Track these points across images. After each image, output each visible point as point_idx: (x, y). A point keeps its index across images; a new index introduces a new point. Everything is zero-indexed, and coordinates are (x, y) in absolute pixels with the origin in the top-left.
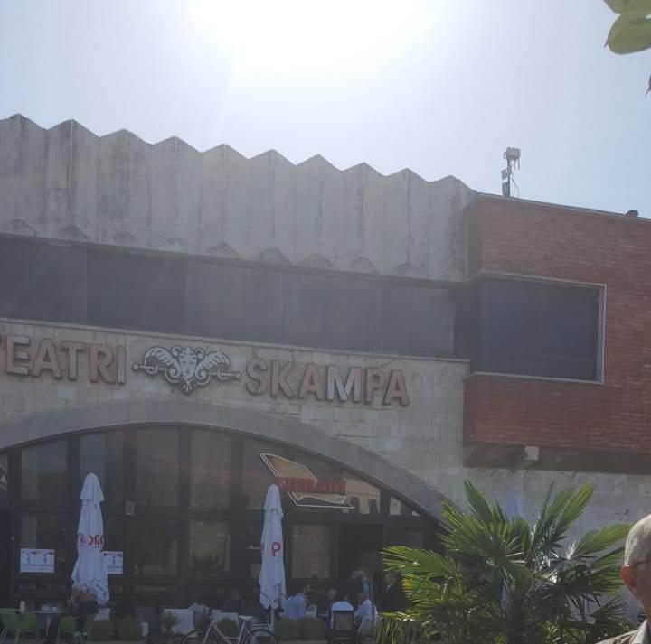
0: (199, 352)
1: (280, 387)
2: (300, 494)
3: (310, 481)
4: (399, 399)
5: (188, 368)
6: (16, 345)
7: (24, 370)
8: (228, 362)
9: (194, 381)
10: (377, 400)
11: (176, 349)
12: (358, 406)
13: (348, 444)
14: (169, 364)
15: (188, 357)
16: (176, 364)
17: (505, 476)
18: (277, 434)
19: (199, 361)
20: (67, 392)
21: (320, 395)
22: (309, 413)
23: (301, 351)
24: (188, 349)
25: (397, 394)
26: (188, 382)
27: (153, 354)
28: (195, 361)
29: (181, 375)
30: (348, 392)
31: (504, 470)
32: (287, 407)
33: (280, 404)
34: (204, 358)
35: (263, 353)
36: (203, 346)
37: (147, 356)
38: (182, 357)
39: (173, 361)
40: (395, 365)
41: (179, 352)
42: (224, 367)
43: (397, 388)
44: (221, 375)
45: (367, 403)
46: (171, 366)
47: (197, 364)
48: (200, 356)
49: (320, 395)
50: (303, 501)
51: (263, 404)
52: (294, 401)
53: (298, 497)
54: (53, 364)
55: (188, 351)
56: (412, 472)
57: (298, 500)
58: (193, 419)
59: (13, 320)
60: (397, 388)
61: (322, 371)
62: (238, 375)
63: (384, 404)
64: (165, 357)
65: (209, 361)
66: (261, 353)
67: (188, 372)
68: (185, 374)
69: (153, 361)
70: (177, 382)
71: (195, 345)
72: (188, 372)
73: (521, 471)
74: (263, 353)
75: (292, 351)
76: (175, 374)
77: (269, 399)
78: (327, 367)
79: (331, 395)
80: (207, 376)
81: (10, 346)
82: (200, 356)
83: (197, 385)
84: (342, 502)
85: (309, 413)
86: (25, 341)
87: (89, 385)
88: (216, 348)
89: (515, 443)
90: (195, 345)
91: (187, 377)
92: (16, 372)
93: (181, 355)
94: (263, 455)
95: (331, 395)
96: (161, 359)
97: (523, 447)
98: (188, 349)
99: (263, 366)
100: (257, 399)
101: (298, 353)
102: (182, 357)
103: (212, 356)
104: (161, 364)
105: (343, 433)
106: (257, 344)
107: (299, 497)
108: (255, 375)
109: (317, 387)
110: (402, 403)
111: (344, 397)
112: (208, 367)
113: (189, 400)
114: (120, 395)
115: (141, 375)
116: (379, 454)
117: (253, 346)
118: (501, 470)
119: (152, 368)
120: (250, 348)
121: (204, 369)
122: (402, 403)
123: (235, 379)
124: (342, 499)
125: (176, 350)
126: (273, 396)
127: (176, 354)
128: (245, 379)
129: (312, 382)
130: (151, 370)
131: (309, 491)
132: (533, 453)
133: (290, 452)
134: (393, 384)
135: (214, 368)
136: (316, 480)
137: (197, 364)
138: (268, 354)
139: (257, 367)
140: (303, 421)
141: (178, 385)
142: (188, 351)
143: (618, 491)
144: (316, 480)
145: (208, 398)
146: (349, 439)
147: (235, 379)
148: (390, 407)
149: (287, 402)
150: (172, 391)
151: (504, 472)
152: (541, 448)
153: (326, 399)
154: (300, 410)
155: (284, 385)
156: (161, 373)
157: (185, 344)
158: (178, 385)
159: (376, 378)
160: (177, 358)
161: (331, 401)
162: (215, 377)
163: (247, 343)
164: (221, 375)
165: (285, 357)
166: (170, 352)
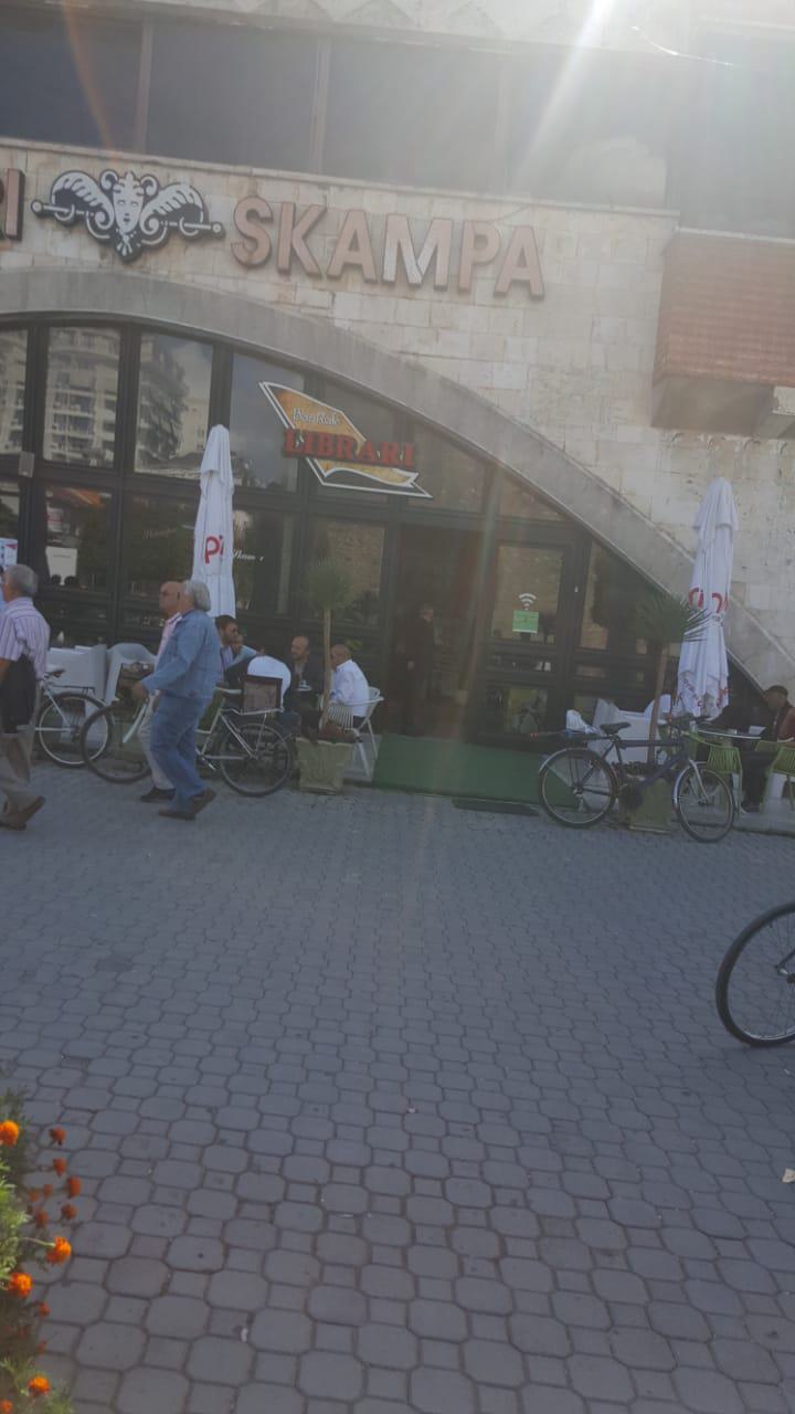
0: (149, 183)
1: (293, 252)
2: (328, 462)
3: (349, 442)
4: (526, 284)
5: (128, 211)
8: (200, 205)
9: (138, 234)
12: (445, 297)
14: (93, 204)
15: (128, 191)
16: (107, 205)
17: (737, 449)
19: (147, 199)
23: (341, 187)
24: (130, 177)
25: (522, 275)
26: (126, 239)
27: (67, 186)
28: (141, 199)
29: (115, 225)
32: (308, 294)
33: (295, 288)
34: (156, 194)
35: (269, 191)
36: (159, 173)
37: (58, 187)
38: (119, 192)
39: (103, 199)
42: (189, 211)
45: (463, 291)
46: (99, 208)
48: (151, 191)
50: (335, 477)
52: (324, 283)
53: (325, 468)
55: (129, 181)
56: (543, 430)
57: (325, 475)
58: (138, 310)
62: (217, 229)
63: (498, 295)
64: (90, 191)
65: (166, 201)
68: (121, 223)
69: (66, 197)
70: (107, 237)
71: (138, 171)
72: (127, 220)
73: (773, 442)
74: (269, 191)
75: (323, 186)
76: (105, 223)
77: (273, 276)
79: (390, 275)
80: (161, 228)
82: (151, 191)
84: (407, 484)
85: (350, 308)
88: (181, 176)
90: (138, 171)
91: (124, 228)
93: (117, 187)
94: (264, 385)
95: (390, 275)
96: (80, 194)
97: (772, 387)
98: (130, 177)
99: (264, 212)
100: (253, 276)
101: (333, 190)
102: (119, 192)
103: (171, 191)
104: (81, 203)
105: (412, 349)
106: (256, 171)
107: (327, 469)
108: (250, 229)
111: (415, 277)
113: (130, 272)
115: (49, 225)
117: (249, 175)
118: (729, 438)
119: (70, 210)
120: (245, 179)
121: (156, 215)
124: (408, 478)
125: (110, 178)
126: (285, 273)
127: (107, 185)
130: (61, 214)
131: (344, 459)
133: (319, 383)
135: (174, 215)
136: (360, 439)
139: (252, 215)
140: (338, 324)
141: (109, 240)
142: (129, 181)
144: (360, 439)
145: (165, 272)
146: (422, 361)
147: (206, 237)
149: (308, 283)
150: (103, 256)
151: (737, 441)
154: (333, 301)
155: (301, 251)
156: (78, 220)
157: (119, 168)
158: (109, 240)
160: (109, 193)
161: (391, 285)
162: (173, 231)
163: (241, 169)
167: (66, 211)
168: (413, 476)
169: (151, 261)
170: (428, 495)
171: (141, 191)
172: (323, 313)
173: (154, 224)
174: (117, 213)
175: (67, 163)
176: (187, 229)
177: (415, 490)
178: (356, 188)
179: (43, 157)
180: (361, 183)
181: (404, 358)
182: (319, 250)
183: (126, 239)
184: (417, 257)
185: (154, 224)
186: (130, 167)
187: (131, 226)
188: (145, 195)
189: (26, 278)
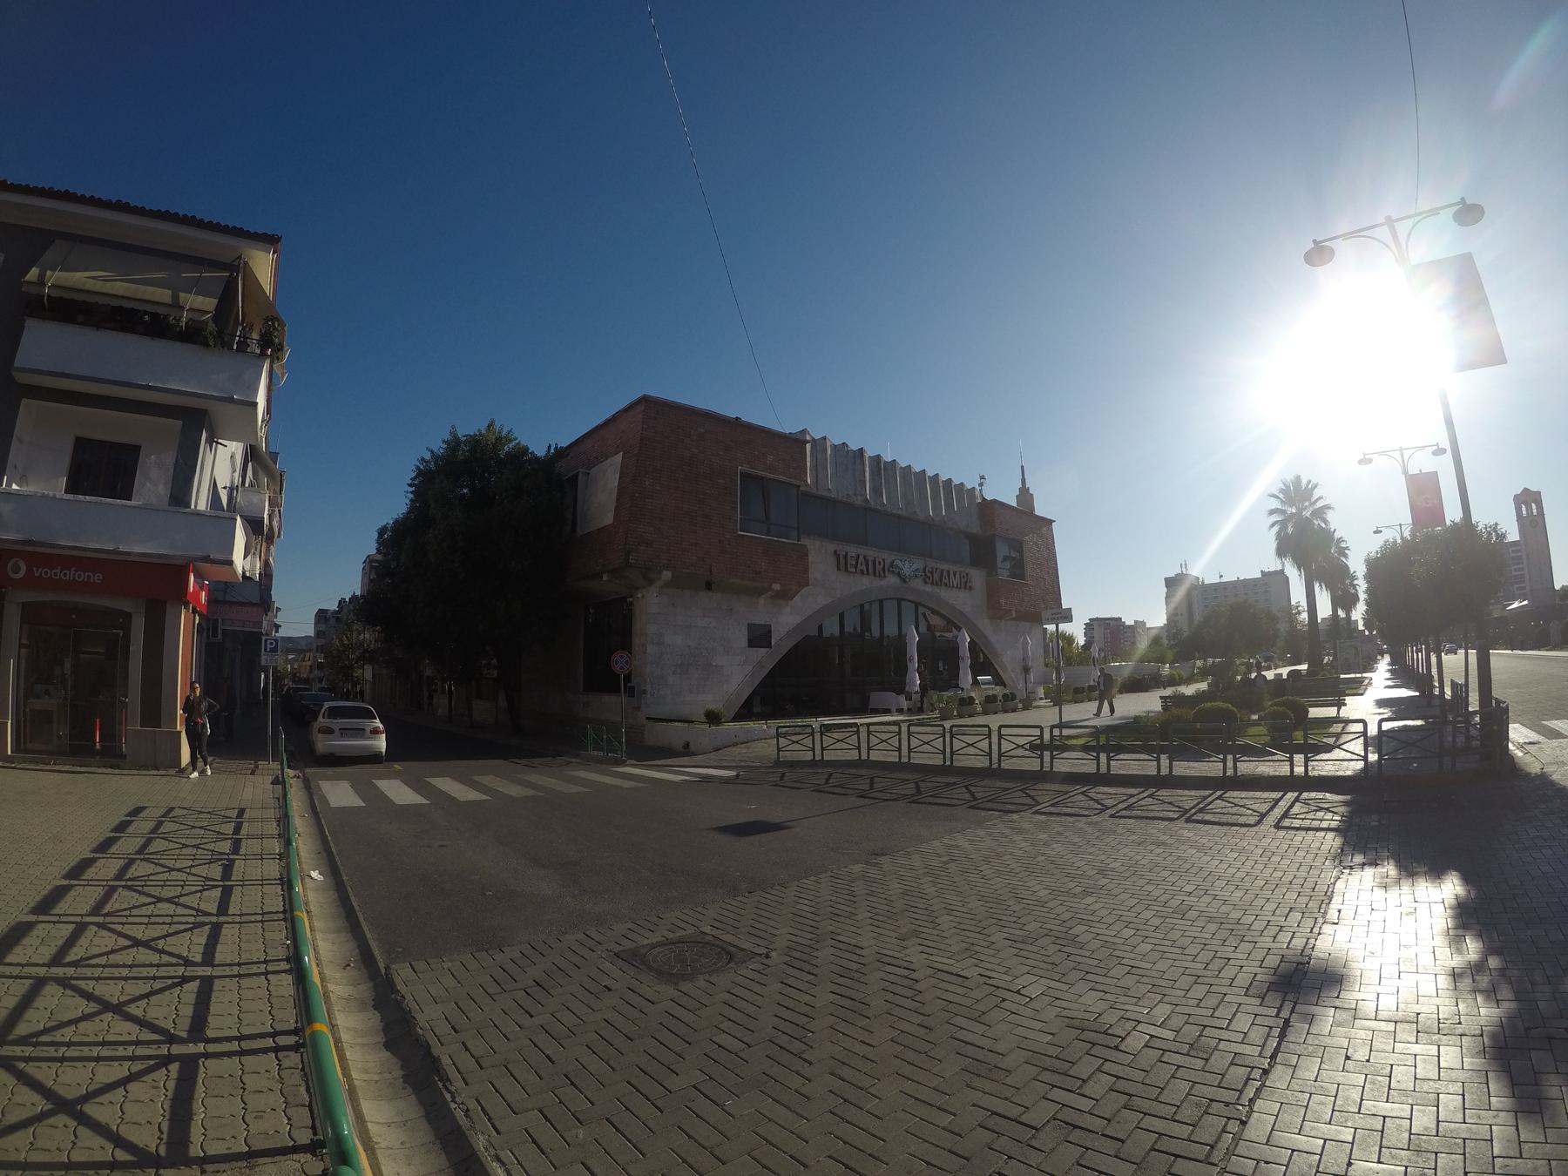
22: (943, 593)
51: (928, 588)
114: (884, 582)
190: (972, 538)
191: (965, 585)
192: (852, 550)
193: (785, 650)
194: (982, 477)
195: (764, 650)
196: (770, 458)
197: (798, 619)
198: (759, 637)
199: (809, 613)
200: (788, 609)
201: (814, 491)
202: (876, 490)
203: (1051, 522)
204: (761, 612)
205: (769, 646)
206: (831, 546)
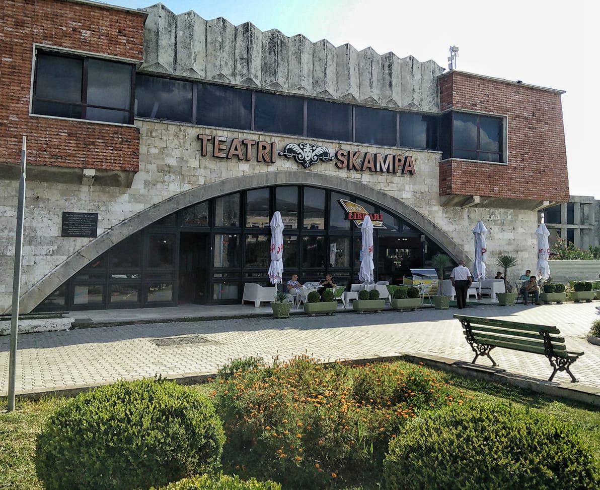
6: (220, 141)
7: (224, 155)
10: (400, 172)
11: (302, 145)
13: (385, 194)
14: (298, 152)
15: (308, 148)
18: (352, 190)
19: (313, 151)
20: (244, 168)
21: (373, 169)
22: (366, 178)
23: (362, 146)
24: (308, 144)
25: (410, 169)
26: (308, 162)
27: (290, 147)
28: (311, 151)
29: (305, 158)
30: (386, 167)
31: (458, 208)
32: (355, 175)
34: (316, 149)
36: (315, 143)
37: (287, 148)
39: (301, 151)
40: (407, 154)
41: (304, 146)
42: (326, 154)
43: (410, 166)
44: (323, 157)
46: (300, 153)
47: (313, 152)
48: (314, 148)
49: (373, 169)
51: (343, 174)
52: (359, 172)
54: (240, 152)
56: (416, 209)
58: (309, 182)
59: (217, 128)
60: (410, 166)
61: (373, 156)
62: (333, 158)
63: (403, 173)
64: (297, 149)
65: (319, 151)
66: (343, 147)
67: (308, 157)
68: (306, 158)
69: (290, 150)
71: (311, 142)
72: (308, 157)
75: (357, 146)
78: (376, 155)
79: (378, 169)
80: (318, 159)
81: (217, 142)
82: (314, 148)
83: (312, 162)
84: (380, 225)
86: (224, 139)
87: (256, 163)
88: (320, 144)
89: (469, 194)
90: (311, 142)
91: (307, 159)
92: (219, 156)
93: (305, 147)
94: (341, 200)
95: (378, 169)
96: (294, 149)
97: (473, 196)
98: (308, 144)
104: (295, 152)
106: (341, 142)
109: (372, 165)
110: (411, 173)
111: (385, 170)
112: (318, 154)
114: (272, 169)
116: (400, 200)
119: (289, 154)
121: (316, 155)
122: (411, 173)
123: (331, 160)
124: (380, 223)
126: (349, 169)
127: (302, 147)
128: (335, 161)
129: (369, 162)
132: (477, 199)
133: (354, 198)
134: (407, 164)
135: (321, 155)
137: (313, 152)
138: (347, 147)
140: (363, 183)
141: (303, 163)
143: (509, 218)
148: (406, 175)
149: (355, 172)
152: (480, 196)
153: (376, 171)
157: (306, 142)
158: (303, 163)
159: (400, 160)
162: (321, 160)
163: (336, 141)
164: (323, 157)
165: (354, 149)
166: (299, 145)
167: (290, 154)
168: (382, 223)
169: (312, 168)
170: (386, 228)
171: (311, 148)
172: (359, 180)
173: (316, 157)
174: (305, 155)
175: (287, 141)
176: (325, 159)
177: (383, 227)
178: (366, 146)
179: (280, 138)
180: (368, 145)
181: (381, 191)
182: (358, 162)
183: (308, 162)
184: (385, 164)
185: (316, 157)
186: (308, 141)
187: (309, 158)
188: (313, 149)
189: (276, 174)
190: (427, 118)
191: (405, 168)
192: (223, 134)
193: (117, 238)
194: (454, 50)
195: (86, 241)
196: (86, 34)
197: (140, 207)
198: (77, 225)
199: (156, 200)
200: (126, 197)
201: (171, 71)
202: (269, 70)
203: (557, 94)
204: (82, 201)
205: (93, 234)
206: (193, 131)
